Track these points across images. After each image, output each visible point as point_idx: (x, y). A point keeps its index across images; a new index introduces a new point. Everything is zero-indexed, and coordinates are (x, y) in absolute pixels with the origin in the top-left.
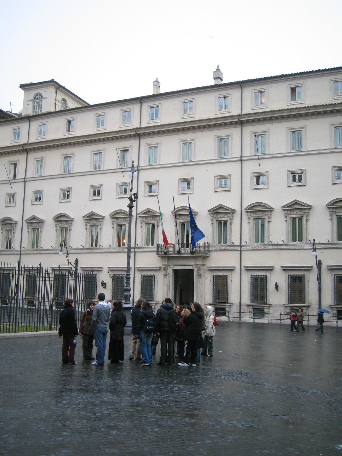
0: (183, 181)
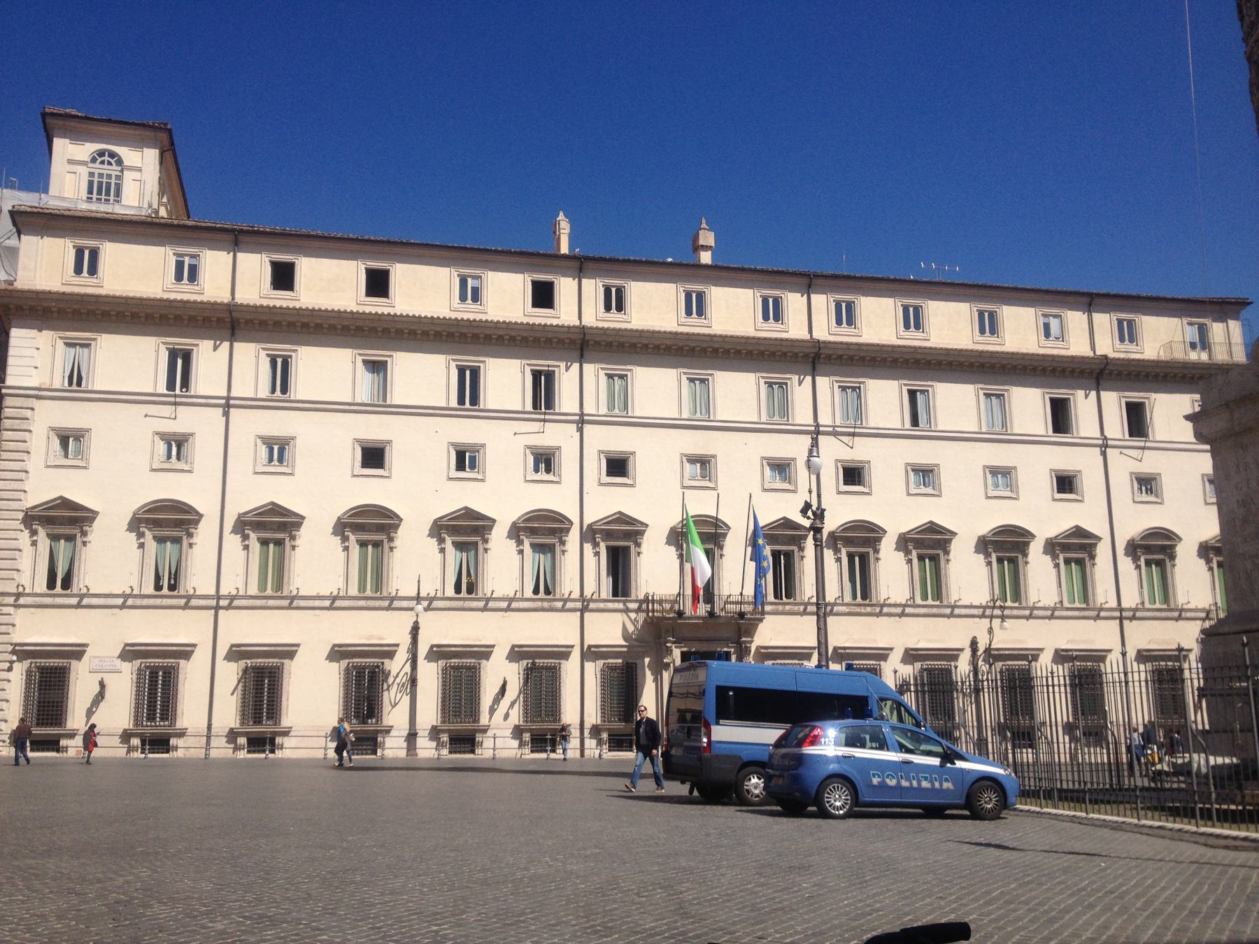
0: (693, 460)
